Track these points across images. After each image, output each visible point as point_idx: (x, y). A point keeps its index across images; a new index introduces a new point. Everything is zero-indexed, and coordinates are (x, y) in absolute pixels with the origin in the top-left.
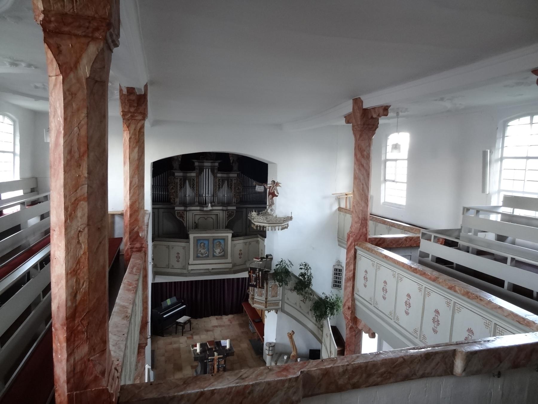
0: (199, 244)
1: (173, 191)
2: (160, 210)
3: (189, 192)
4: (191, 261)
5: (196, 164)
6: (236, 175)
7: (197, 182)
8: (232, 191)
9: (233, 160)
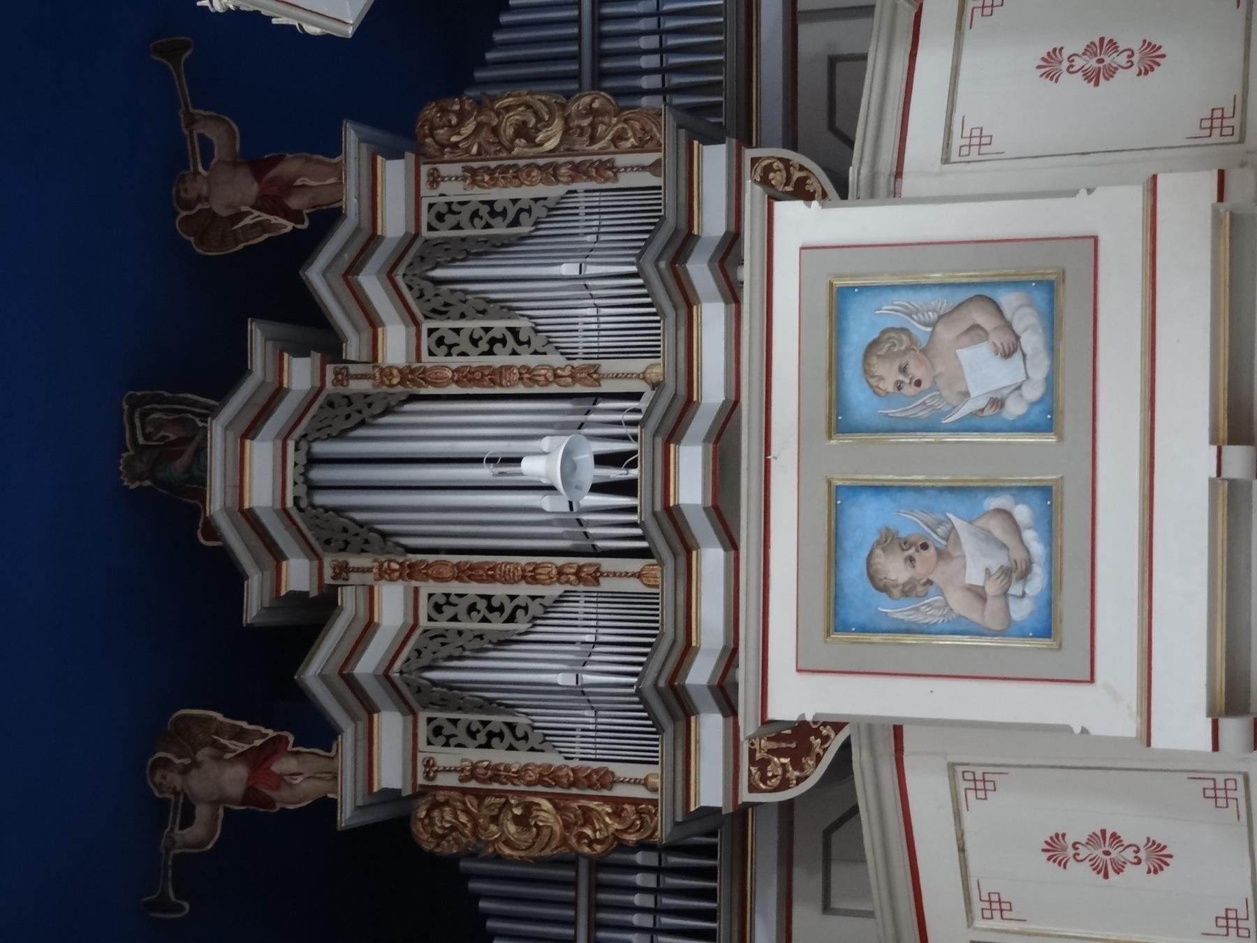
0: (900, 611)
3: (566, 662)
4: (1103, 710)
5: (298, 574)
6: (394, 173)
7: (463, 574)
8: (554, 209)
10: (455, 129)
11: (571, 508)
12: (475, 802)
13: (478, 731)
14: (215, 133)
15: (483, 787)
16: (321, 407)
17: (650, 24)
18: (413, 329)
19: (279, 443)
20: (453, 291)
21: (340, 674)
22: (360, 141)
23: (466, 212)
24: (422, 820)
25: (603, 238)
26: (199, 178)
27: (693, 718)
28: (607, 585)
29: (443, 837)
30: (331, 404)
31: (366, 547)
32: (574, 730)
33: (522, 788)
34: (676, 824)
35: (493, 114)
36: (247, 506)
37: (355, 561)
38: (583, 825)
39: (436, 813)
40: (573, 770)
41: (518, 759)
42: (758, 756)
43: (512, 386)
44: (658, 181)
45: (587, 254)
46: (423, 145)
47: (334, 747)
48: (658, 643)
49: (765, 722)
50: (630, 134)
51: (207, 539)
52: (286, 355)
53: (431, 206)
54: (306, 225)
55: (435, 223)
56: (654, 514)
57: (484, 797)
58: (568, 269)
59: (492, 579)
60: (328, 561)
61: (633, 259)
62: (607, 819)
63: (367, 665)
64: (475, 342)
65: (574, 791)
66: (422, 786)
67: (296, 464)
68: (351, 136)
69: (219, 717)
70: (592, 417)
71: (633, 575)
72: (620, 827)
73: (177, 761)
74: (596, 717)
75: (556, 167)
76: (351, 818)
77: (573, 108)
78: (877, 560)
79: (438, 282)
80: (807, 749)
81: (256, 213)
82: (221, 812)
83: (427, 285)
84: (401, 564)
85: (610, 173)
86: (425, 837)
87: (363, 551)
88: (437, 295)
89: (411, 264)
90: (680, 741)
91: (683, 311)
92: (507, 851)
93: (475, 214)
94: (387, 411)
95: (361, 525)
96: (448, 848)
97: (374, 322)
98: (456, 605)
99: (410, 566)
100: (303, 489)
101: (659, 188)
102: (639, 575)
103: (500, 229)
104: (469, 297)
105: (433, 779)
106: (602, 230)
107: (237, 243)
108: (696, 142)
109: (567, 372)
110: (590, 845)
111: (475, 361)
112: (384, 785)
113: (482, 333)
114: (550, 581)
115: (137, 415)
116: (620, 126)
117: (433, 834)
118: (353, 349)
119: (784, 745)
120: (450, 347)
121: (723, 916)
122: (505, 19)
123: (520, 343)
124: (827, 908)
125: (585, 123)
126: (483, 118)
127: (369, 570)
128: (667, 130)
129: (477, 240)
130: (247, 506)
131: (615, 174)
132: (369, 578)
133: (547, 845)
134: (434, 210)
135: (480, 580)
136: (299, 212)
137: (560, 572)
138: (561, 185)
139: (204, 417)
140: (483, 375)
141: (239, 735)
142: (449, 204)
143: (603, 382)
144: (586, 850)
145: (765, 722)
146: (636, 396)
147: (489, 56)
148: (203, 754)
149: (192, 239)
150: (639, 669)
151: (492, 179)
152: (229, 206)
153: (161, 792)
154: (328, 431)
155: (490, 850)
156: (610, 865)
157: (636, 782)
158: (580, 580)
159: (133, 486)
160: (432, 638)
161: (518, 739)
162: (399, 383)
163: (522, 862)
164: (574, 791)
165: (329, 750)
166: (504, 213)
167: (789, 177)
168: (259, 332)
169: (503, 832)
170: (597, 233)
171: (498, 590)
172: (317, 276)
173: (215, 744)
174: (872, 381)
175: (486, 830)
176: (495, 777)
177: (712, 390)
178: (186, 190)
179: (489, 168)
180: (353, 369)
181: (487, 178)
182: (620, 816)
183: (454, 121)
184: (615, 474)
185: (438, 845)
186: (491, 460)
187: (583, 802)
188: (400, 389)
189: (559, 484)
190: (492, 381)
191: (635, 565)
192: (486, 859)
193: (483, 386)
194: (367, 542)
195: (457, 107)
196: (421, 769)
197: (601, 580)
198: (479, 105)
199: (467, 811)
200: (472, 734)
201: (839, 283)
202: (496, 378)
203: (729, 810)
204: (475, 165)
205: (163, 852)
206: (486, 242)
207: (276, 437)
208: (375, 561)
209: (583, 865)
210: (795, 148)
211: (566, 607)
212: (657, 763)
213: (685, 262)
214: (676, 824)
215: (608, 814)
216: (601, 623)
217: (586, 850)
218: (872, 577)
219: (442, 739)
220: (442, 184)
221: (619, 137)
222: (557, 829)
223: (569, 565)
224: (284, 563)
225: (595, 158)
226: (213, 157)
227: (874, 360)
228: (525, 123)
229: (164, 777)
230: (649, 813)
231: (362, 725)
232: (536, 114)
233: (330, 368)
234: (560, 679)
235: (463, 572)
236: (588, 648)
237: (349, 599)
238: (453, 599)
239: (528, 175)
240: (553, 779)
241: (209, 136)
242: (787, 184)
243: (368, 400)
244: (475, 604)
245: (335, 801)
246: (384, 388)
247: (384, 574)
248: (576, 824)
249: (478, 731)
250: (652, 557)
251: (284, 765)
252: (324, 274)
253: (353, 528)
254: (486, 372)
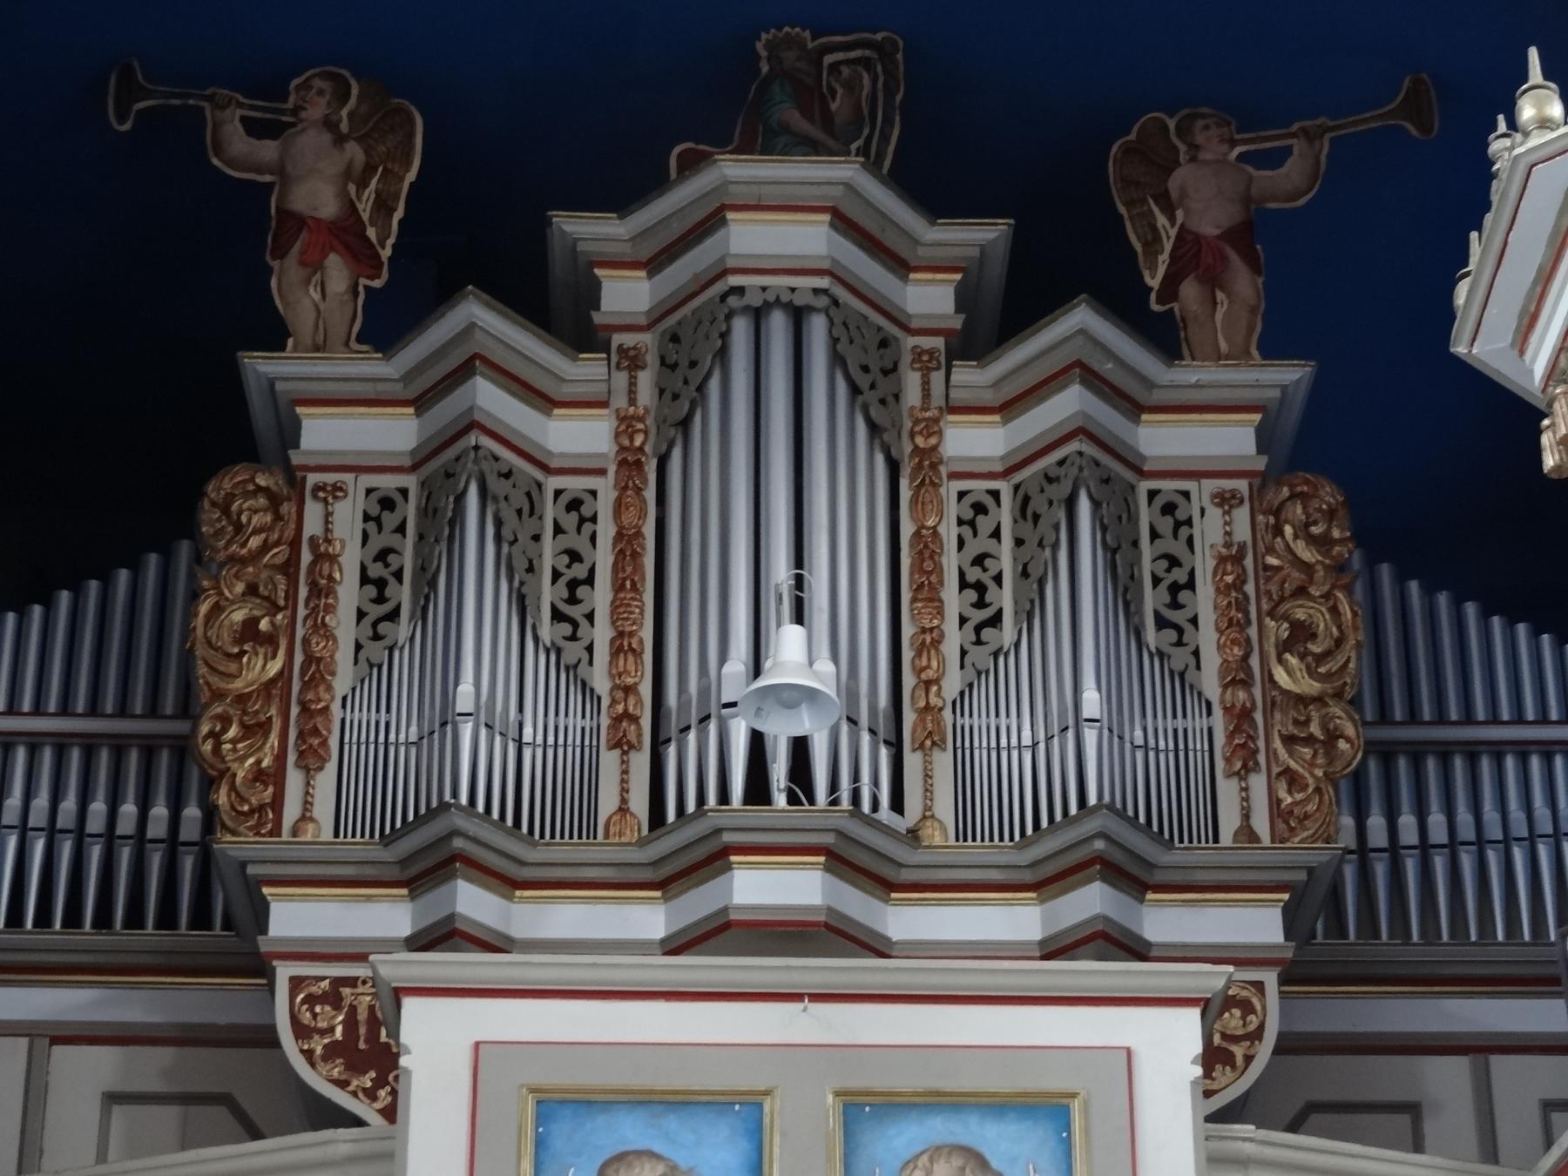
1: (263, 668)
2: (58, 1050)
3: (491, 697)
5: (626, 295)
6: (1233, 440)
7: (626, 543)
8: (1183, 681)
9: (1185, 237)
10: (1303, 530)
11: (727, 706)
12: (279, 560)
13: (387, 565)
14: (1293, 172)
15: (301, 573)
16: (880, 329)
17: (1466, 831)
18: (999, 468)
19: (826, 265)
20: (1057, 527)
21: (476, 356)
22: (1284, 388)
23: (1178, 549)
24: (252, 480)
25: (1139, 755)
26: (1225, 147)
27: (404, 891)
28: (609, 761)
29: (226, 511)
30: (884, 343)
31: (668, 395)
32: (388, 711)
33: (300, 632)
34: (243, 865)
35: (1327, 588)
36: (730, 216)
37: (646, 379)
38: (243, 725)
39: (262, 501)
40: (327, 708)
41: (344, 625)
42: (346, 991)
43: (913, 617)
44: (1226, 838)
45: (1114, 730)
46: (1279, 484)
47: (365, 348)
48: (521, 838)
49: (398, 994)
50: (1299, 796)
51: (679, 155)
52: (958, 277)
53: (1186, 495)
54: (1155, 307)
55: (1159, 501)
56: (718, 831)
57: (286, 574)
58: (1092, 703)
59: (618, 587)
60: (646, 339)
61: (1107, 799)
62: (251, 760)
63: (487, 396)
64: (979, 561)
65: (295, 710)
66: (304, 479)
67: (793, 290)
68: (1292, 374)
69: (411, 176)
70: (866, 738)
71: (624, 801)
72: (239, 780)
73: (344, 113)
74: (407, 744)
75: (1246, 684)
76: (256, 371)
77: (1336, 710)
78: (647, 1166)
79: (1071, 504)
80: (356, 1065)
81: (1173, 232)
82: (268, 178)
83: (1065, 489)
84: (641, 449)
85: (1239, 765)
86: (227, 485)
87: (662, 392)
88: (1051, 503)
89: (1097, 464)
90: (369, 872)
91: (1028, 877)
92: (204, 608)
93: (1174, 562)
94: (874, 428)
95: (701, 388)
96: (209, 520)
97: (1008, 408)
98: (579, 531)
99: (638, 464)
100: (755, 300)
101: (1216, 840)
102: (623, 809)
103: (1151, 600)
104: (1048, 552)
105: (315, 497)
106: (1152, 754)
107: (1129, 204)
108: (1286, 896)
109: (933, 700)
110: (211, 734)
111: (951, 562)
112: (305, 423)
113: (993, 572)
114: (615, 674)
115: (867, 53)
116: (1311, 781)
117: (231, 497)
118: (969, 378)
119: (362, 1030)
120: (972, 523)
121: (102, 939)
122: (1471, 609)
123: (978, 629)
124: (113, 1099)
125: (1315, 729)
126: (1320, 573)
127: (632, 401)
128: (1304, 852)
129: (1135, 563)
130: (730, 216)
131: (1238, 773)
132: (620, 401)
133: (213, 669)
134: (1179, 500)
135: (616, 568)
136: (1174, 296)
137: (628, 690)
138: (1219, 690)
139: (864, 151)
140: (931, 573)
141: (383, 206)
142: (1189, 522)
143: (918, 756)
144: (205, 729)
145: (398, 994)
146: (897, 805)
147: (1414, 586)
148: (355, 152)
149: (1132, 136)
150: (481, 808)
151: (1228, 586)
152: (1183, 194)
153: (298, 88)
154: (844, 340)
155: (206, 583)
156: (181, 767)
157: (307, 804)
158: (617, 720)
159: (759, 46)
160: (529, 495)
161: (375, 625)
162: (916, 447)
163: (188, 631)
164: (295, 710)
165: (359, 340)
166: (1175, 605)
167: (1236, 1039)
168: (993, 235)
169: (233, 602)
170: (1146, 747)
171: (601, 596)
172: (1081, 318)
173: (369, 169)
174: (925, 1158)
175: (237, 576)
176: (316, 591)
177: (905, 921)
178: (1207, 127)
179: (1244, 582)
180: (937, 378)
181: (1229, 579)
182: (255, 779)
183: (1315, 530)
184: (779, 772)
185: (214, 504)
186: (799, 582)
187: (277, 724)
188: (908, 448)
189: (762, 682)
190: (920, 587)
191: (640, 803)
192: (191, 576)
193: (912, 574)
194: (676, 397)
195: (1336, 534)
196: (330, 478)
197: (617, 753)
198: (1340, 568)
199: (265, 547)
200: (382, 556)
201: (1076, 1106)
202: (925, 593)
203: (264, 946)
204: (1249, 562)
205: (208, 92)
206: (1132, 577)
207: (834, 261)
208: (647, 410)
209: (180, 727)
210: (1278, 1050)
211: (576, 699)
212: (336, 835)
213: (1104, 880)
214: (243, 865)
215: (259, 762)
216: (550, 752)
217: (205, 729)
218: (621, 1158)
219: (375, 510)
220: (1219, 511)
221: (1293, 780)
222: (238, 685)
223: (639, 702)
224: (643, 274)
225: (1261, 743)
226: (1258, 168)
227: (957, 1162)
228: (1314, 636)
229: (320, 93)
230: (260, 824)
231: (397, 390)
232: (1327, 654)
233: (938, 342)
234: (466, 688)
235: (629, 542)
236: (513, 732)
237: (588, 370)
238: (587, 527)
239: (1234, 642)
240: (312, 678)
241: (1290, 162)
242: (1224, 1036)
243: (890, 399)
244: (580, 560)
245: (283, 348)
246: (908, 424)
247: (626, 425)
248: (245, 713)
249: (387, 565)
250: (652, 828)
251: (337, 271)
252: (1082, 332)
253: (696, 377)
254: (933, 578)
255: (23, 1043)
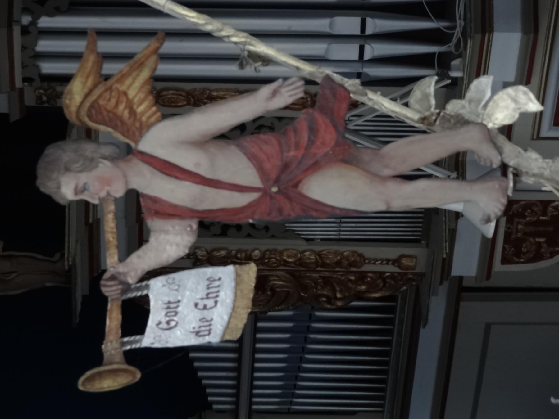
42: (513, 237)
119: (541, 229)
255: (462, 304)
